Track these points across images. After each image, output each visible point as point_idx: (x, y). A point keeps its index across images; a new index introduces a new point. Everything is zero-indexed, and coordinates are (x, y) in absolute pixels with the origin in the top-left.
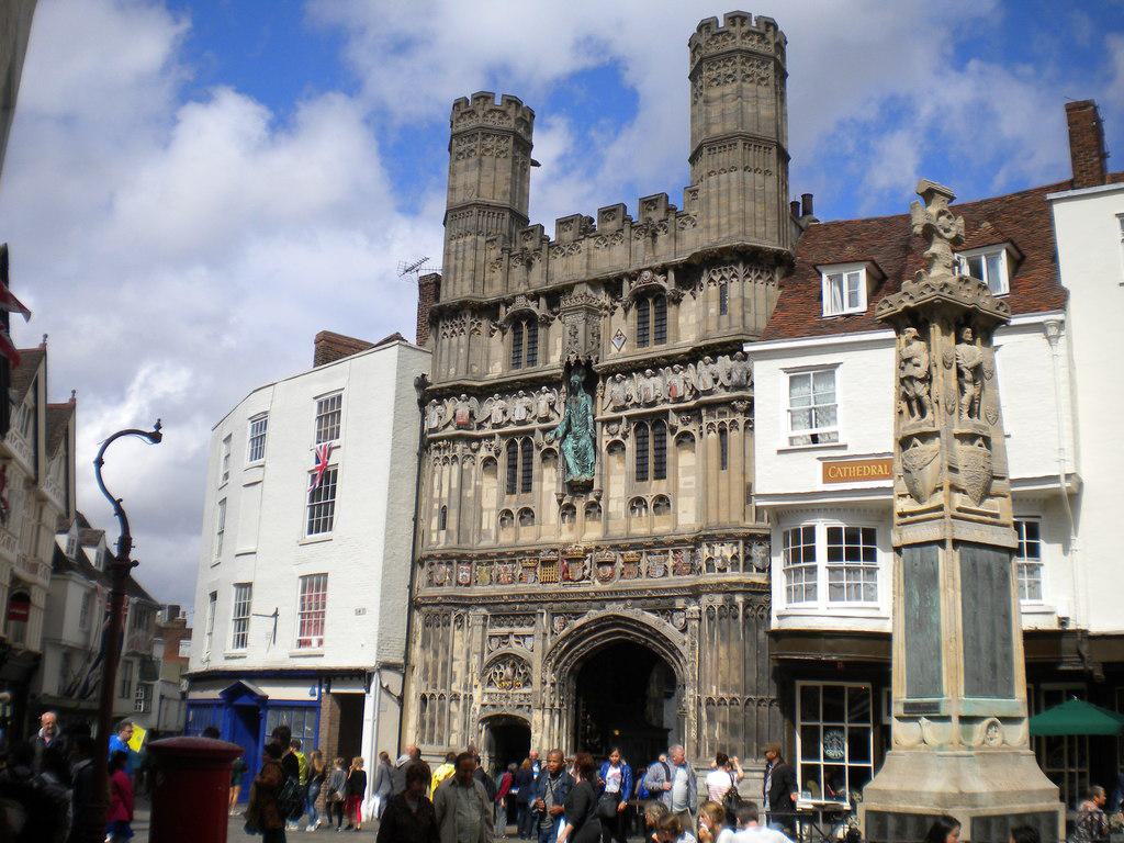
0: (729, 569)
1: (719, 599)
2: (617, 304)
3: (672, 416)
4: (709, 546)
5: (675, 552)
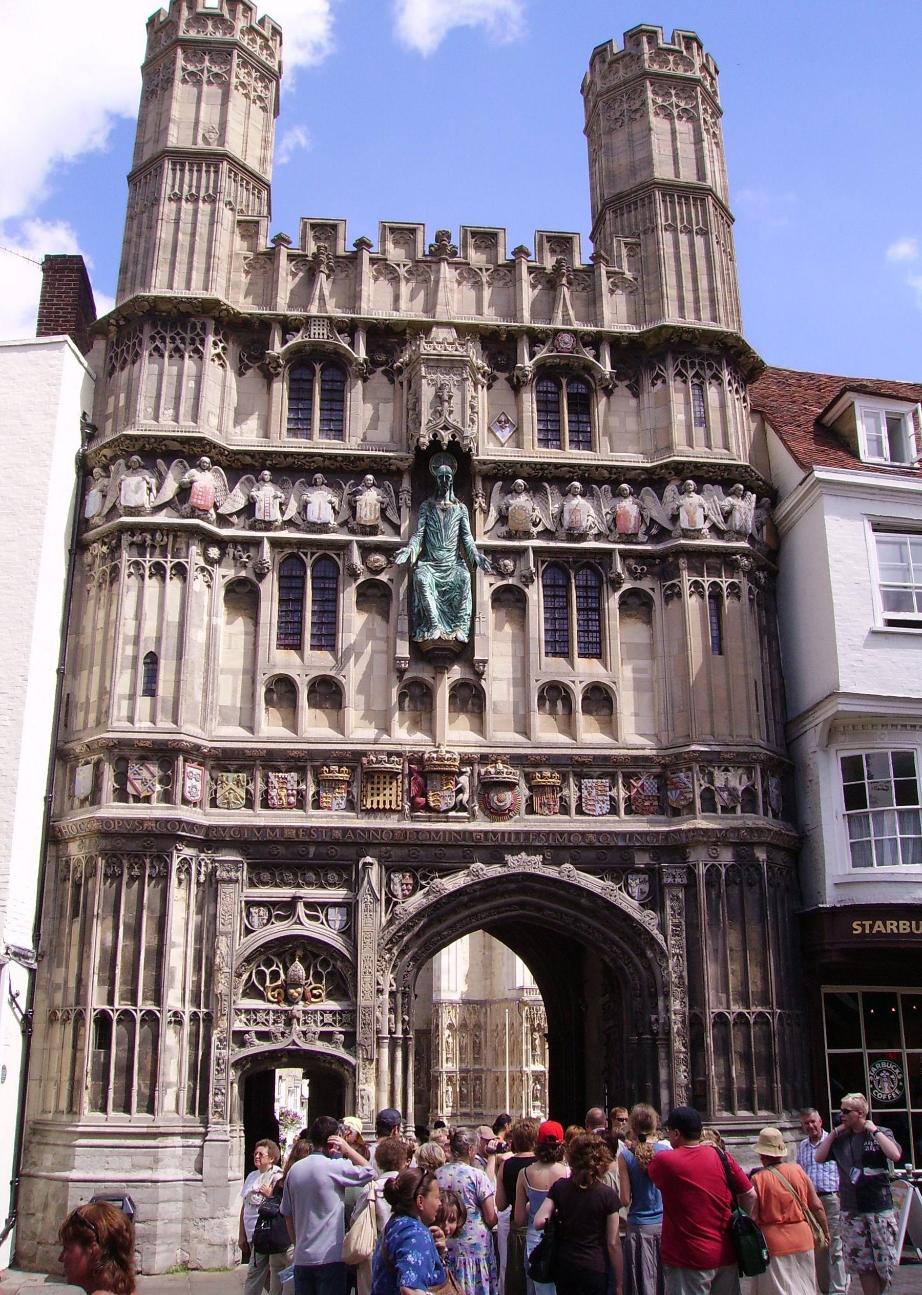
0: (739, 808)
1: (726, 857)
2: (498, 374)
3: (619, 567)
4: (702, 770)
5: (627, 777)
